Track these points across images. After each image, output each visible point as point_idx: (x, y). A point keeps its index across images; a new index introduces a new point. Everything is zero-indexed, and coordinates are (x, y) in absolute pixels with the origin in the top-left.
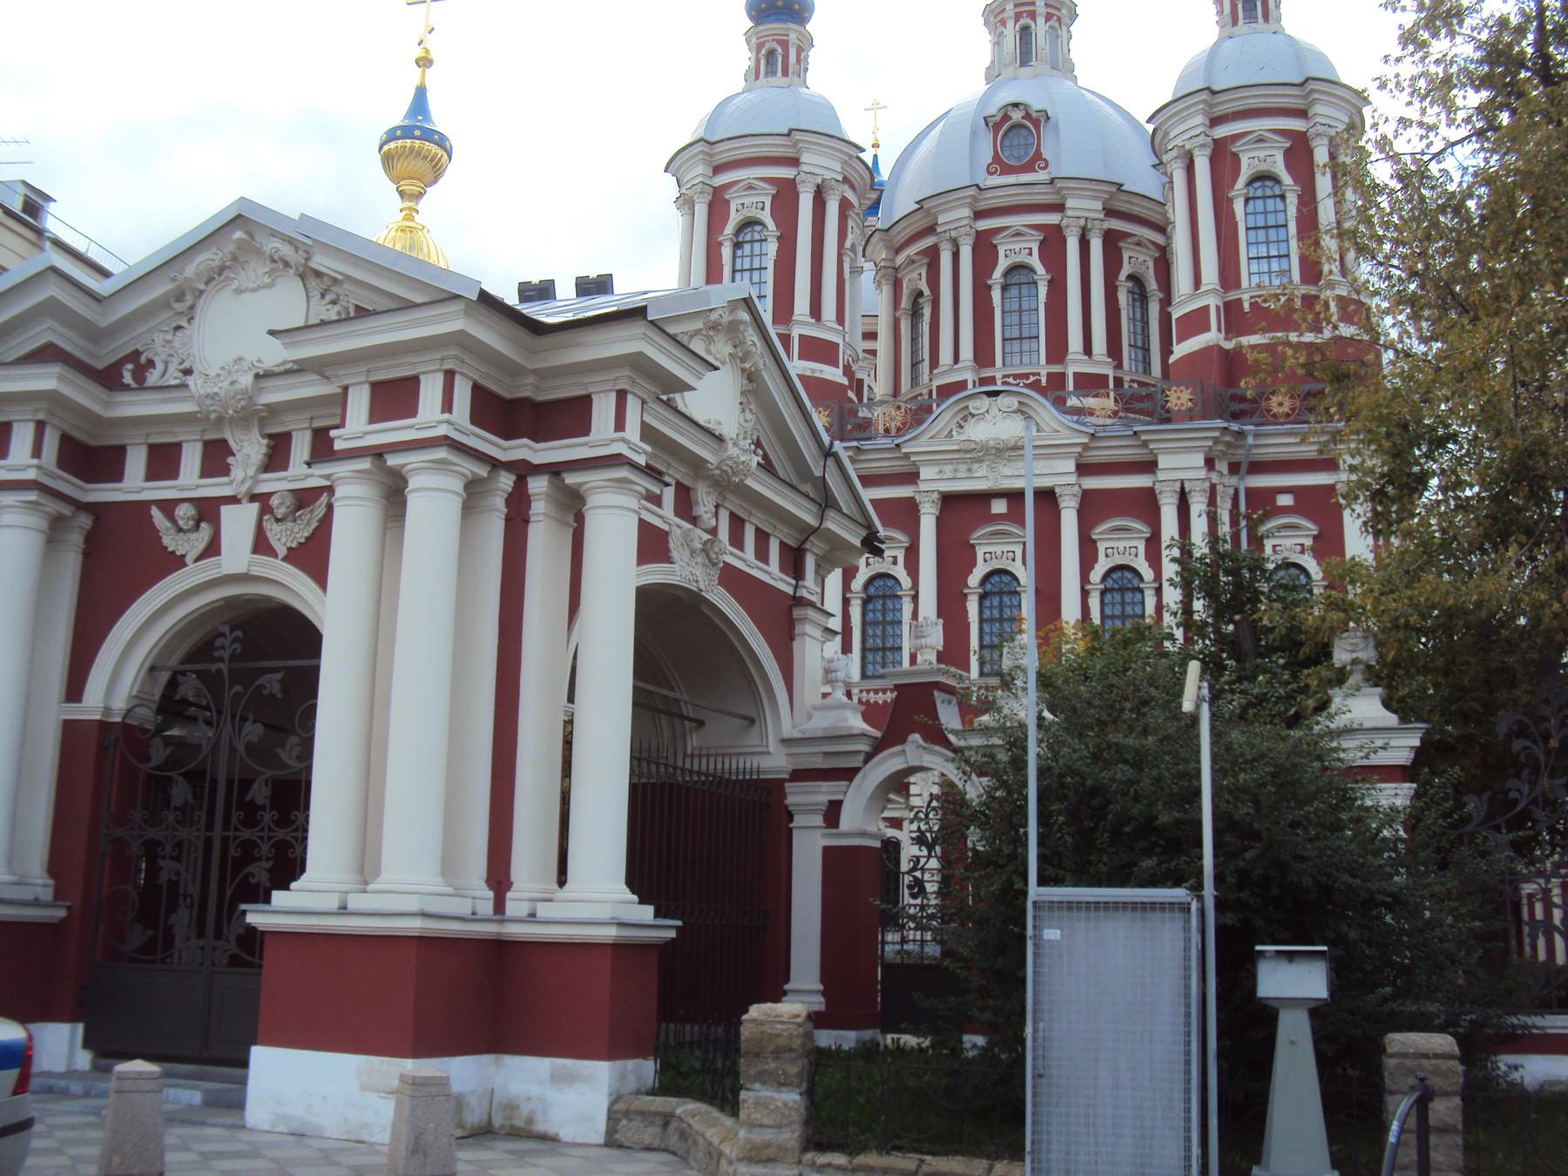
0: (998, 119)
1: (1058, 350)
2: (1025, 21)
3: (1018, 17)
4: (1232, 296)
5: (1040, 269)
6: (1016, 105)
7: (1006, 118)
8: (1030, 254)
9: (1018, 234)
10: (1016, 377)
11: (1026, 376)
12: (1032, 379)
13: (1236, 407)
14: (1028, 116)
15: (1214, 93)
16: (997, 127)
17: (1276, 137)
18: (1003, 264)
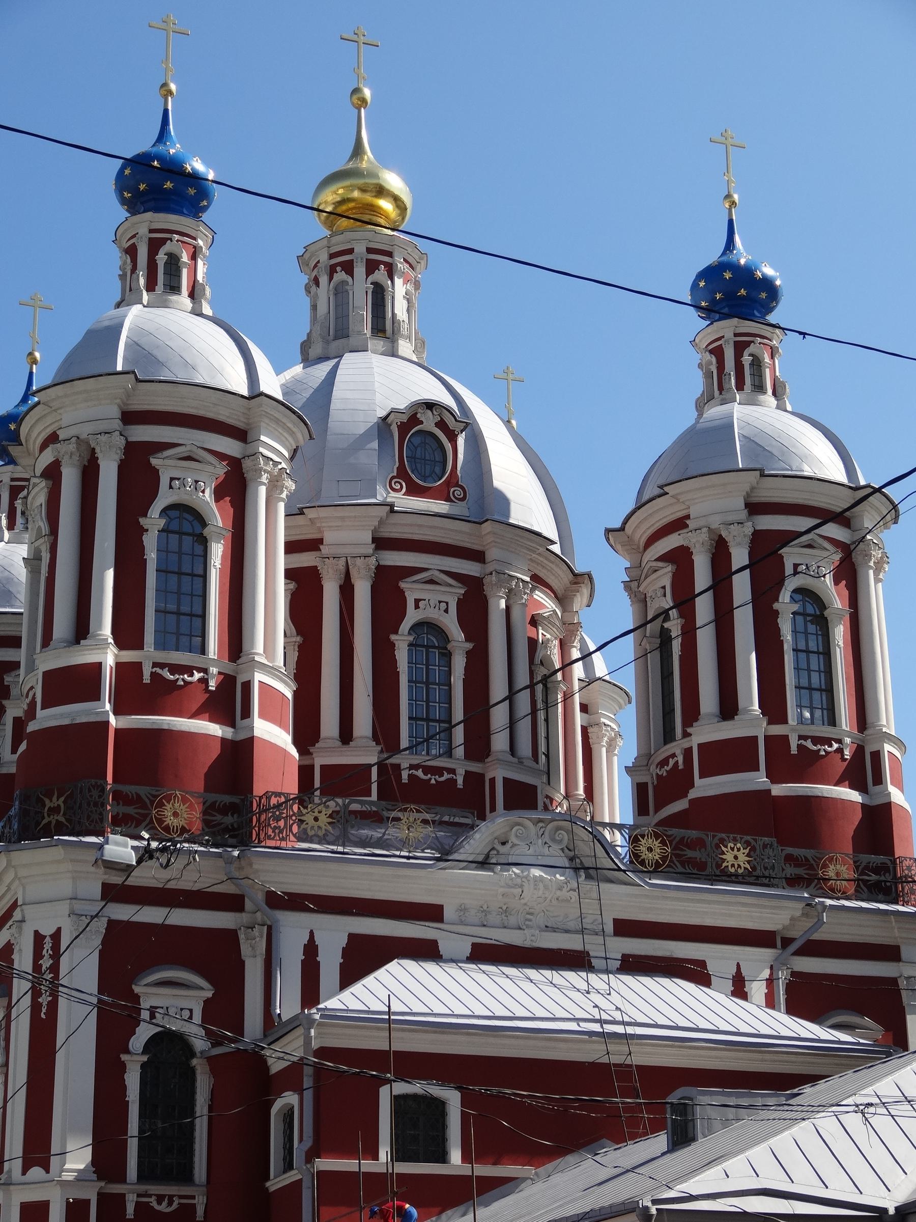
0: (404, 418)
1: (479, 746)
2: (380, 275)
3: (371, 267)
4: (777, 730)
5: (456, 634)
6: (430, 405)
7: (414, 420)
8: (446, 611)
9: (431, 582)
10: (427, 770)
11: (439, 771)
12: (446, 776)
13: (790, 871)
14: (442, 425)
15: (763, 475)
16: (404, 428)
17: (826, 545)
18: (412, 616)
